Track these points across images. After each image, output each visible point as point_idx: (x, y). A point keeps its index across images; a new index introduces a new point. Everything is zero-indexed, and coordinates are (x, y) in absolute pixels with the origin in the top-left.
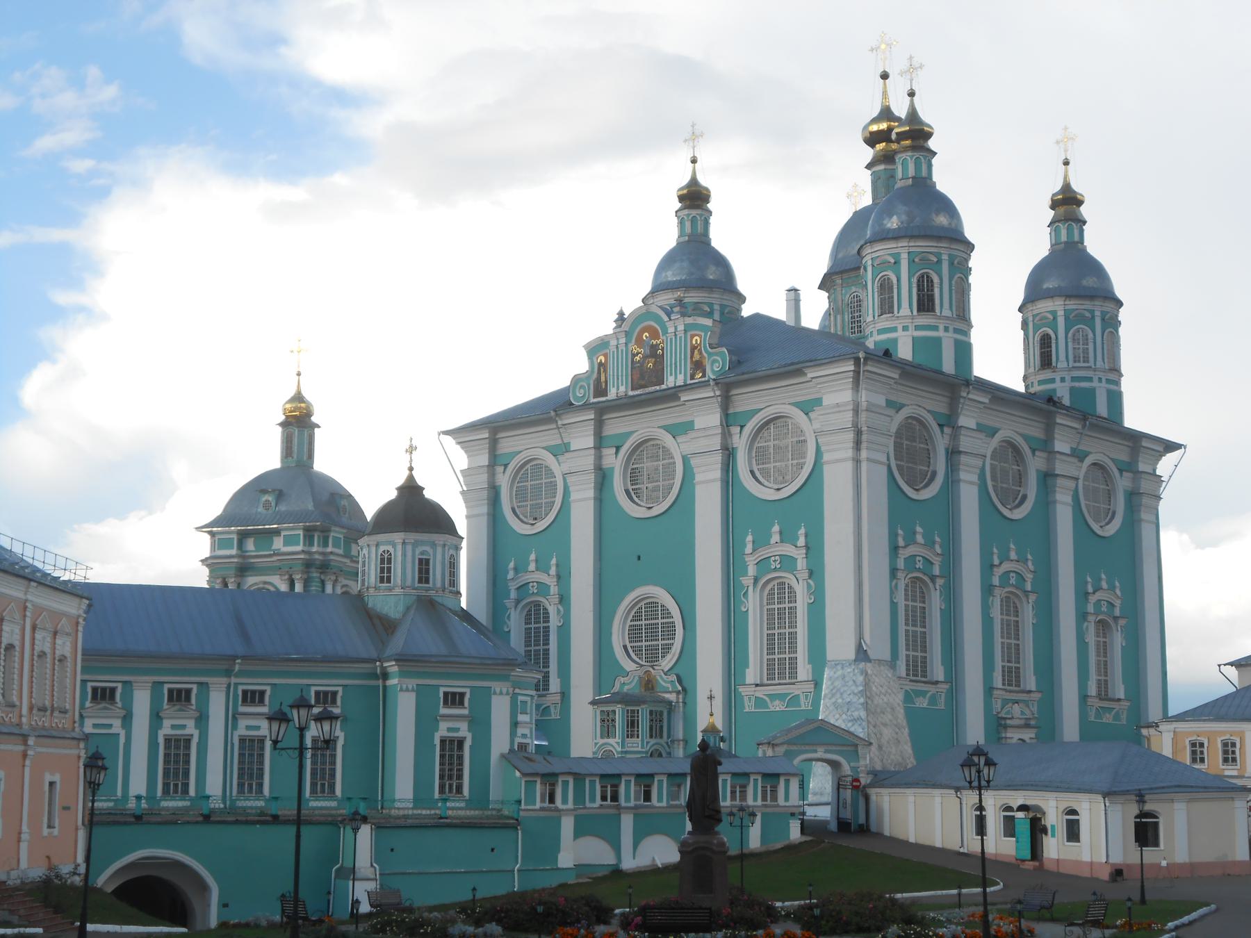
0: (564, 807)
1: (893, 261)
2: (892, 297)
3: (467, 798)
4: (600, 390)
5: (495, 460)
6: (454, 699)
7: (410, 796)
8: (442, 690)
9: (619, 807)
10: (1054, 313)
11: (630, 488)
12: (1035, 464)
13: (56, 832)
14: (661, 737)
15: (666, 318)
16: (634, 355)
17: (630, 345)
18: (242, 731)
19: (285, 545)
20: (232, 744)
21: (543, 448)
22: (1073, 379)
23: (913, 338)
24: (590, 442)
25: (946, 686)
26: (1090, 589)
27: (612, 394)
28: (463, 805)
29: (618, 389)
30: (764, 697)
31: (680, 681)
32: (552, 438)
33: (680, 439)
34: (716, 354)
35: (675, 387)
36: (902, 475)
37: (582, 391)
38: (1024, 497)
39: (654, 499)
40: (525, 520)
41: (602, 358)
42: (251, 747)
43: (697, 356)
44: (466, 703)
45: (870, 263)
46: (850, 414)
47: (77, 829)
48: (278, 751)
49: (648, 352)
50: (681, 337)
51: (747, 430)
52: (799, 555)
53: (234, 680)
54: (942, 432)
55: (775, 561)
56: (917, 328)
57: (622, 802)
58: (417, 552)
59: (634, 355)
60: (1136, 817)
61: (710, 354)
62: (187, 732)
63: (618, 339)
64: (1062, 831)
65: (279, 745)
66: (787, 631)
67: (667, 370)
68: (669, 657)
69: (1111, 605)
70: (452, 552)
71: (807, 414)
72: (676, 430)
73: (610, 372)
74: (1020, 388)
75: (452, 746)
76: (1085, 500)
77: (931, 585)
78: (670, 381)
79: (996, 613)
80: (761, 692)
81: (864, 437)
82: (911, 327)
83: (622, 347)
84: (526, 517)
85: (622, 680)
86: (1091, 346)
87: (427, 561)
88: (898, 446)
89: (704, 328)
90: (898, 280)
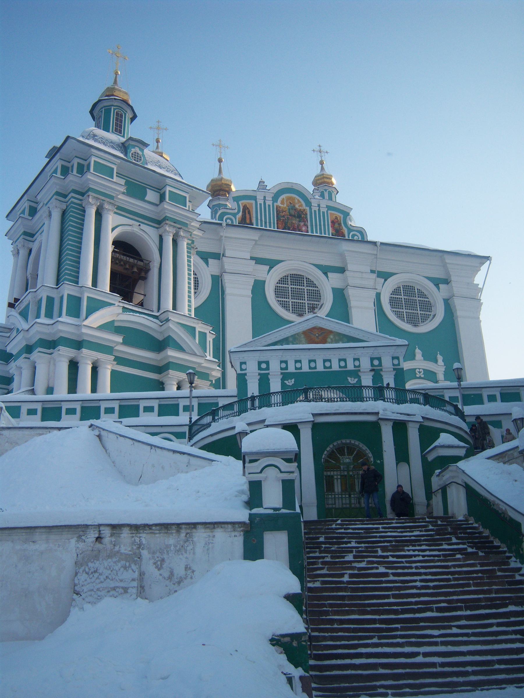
17: (275, 204)
55: (420, 372)
63: (265, 197)
83: (269, 202)
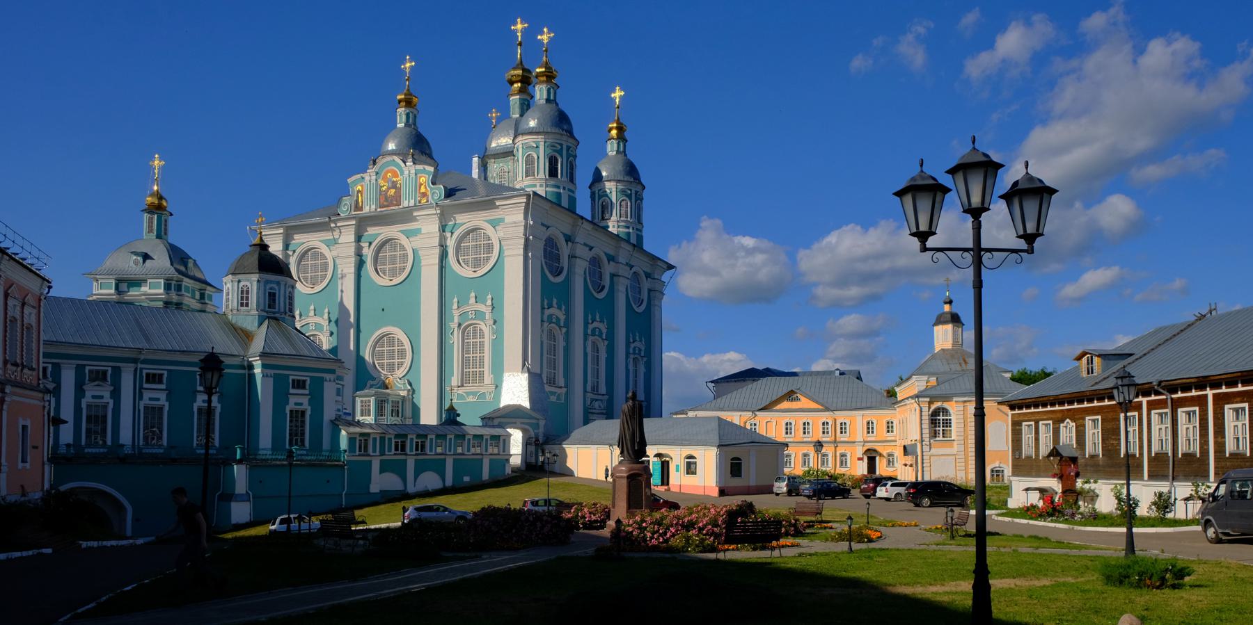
0: (374, 454)
1: (535, 146)
3: (308, 448)
6: (299, 384)
7: (270, 446)
8: (291, 378)
9: (406, 454)
13: (28, 465)
14: (398, 416)
15: (403, 165)
16: (381, 187)
18: (146, 401)
20: (139, 411)
21: (320, 241)
24: (352, 238)
25: (565, 389)
26: (632, 341)
27: (366, 209)
28: (305, 452)
29: (370, 207)
30: (464, 394)
31: (410, 384)
32: (327, 236)
33: (411, 239)
34: (435, 189)
35: (409, 207)
37: (346, 207)
38: (603, 287)
39: (393, 273)
40: (307, 285)
41: (360, 188)
42: (153, 413)
43: (423, 190)
44: (307, 387)
45: (521, 146)
46: (523, 228)
47: (43, 464)
48: (930, 253)
49: (390, 185)
50: (412, 178)
51: (455, 235)
52: (485, 308)
53: (140, 366)
54: (567, 244)
57: (408, 450)
58: (268, 287)
59: (381, 187)
60: (731, 460)
61: (431, 188)
62: (104, 400)
63: (370, 176)
64: (683, 468)
65: (931, 242)
66: (478, 355)
68: (402, 369)
69: (640, 350)
70: (290, 289)
71: (494, 227)
72: (408, 234)
73: (365, 196)
75: (298, 415)
76: (631, 291)
77: (559, 332)
78: (405, 203)
79: (589, 350)
80: (461, 391)
84: (307, 283)
85: (372, 382)
87: (274, 294)
88: (545, 250)
89: (428, 173)
90: (538, 158)
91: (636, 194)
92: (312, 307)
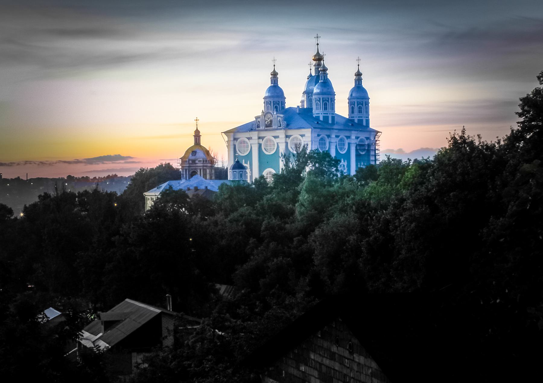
2: (318, 107)
4: (258, 127)
5: (235, 139)
10: (354, 102)
11: (265, 148)
12: (347, 141)
19: (199, 162)
22: (359, 117)
23: (323, 116)
34: (284, 123)
36: (320, 148)
56: (324, 114)
67: (273, 125)
72: (276, 137)
74: (348, 117)
78: (274, 127)
81: (313, 143)
82: (323, 114)
83: (263, 118)
86: (362, 110)
88: (319, 143)
91: (365, 103)
92: (244, 161)
